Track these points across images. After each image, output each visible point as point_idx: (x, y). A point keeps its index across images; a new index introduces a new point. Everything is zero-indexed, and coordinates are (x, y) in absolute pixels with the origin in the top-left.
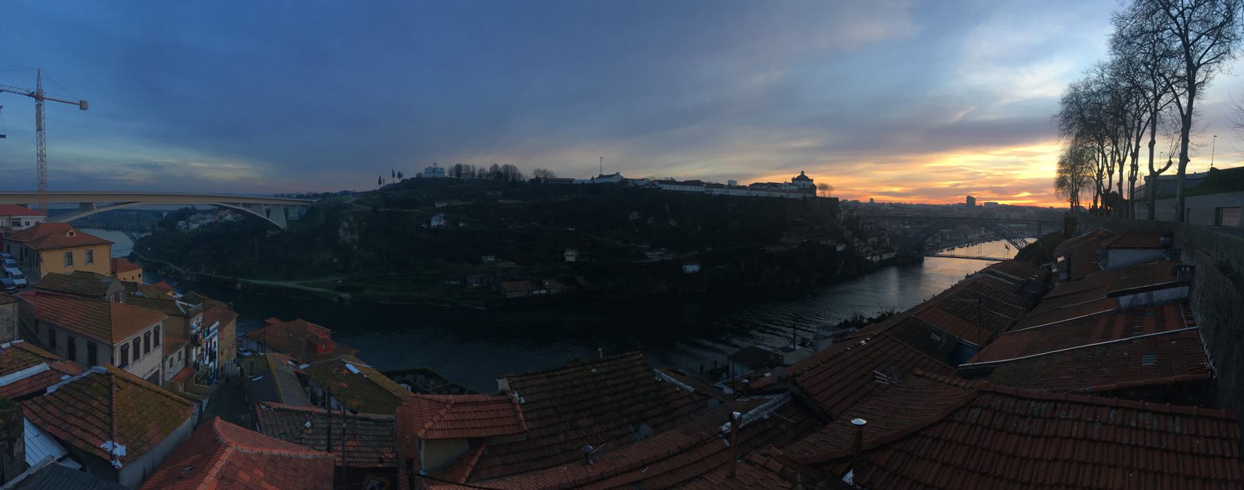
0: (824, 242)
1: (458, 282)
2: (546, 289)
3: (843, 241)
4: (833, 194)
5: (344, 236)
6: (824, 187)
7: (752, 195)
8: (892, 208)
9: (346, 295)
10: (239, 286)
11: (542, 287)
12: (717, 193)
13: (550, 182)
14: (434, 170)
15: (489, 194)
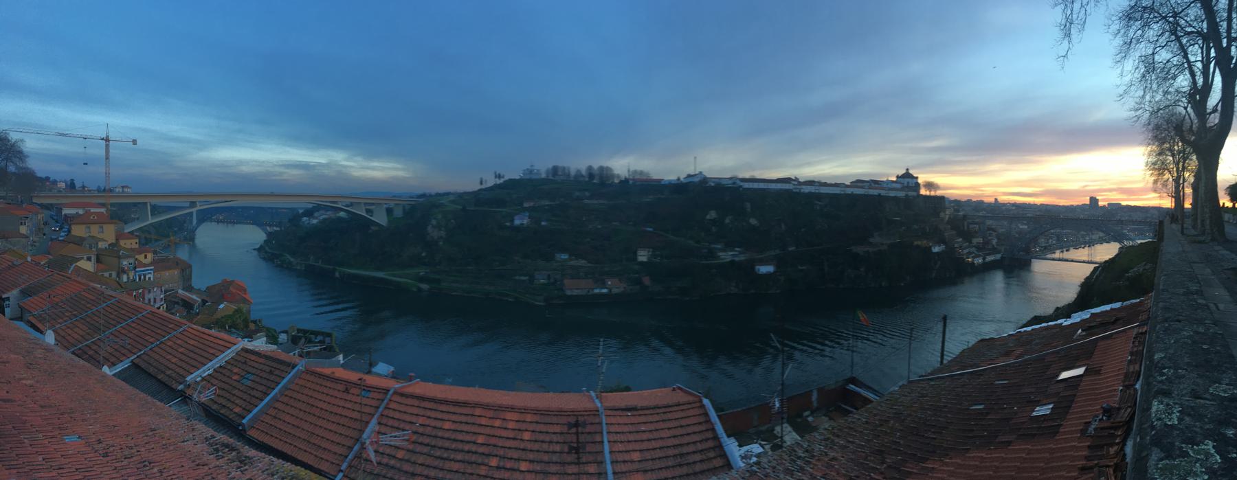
0: (919, 243)
1: (527, 278)
2: (607, 288)
3: (942, 241)
4: (939, 193)
5: (433, 233)
6: (930, 185)
7: (847, 192)
8: (1014, 208)
9: (425, 286)
10: (337, 274)
11: (604, 285)
12: (807, 191)
13: (638, 183)
14: (531, 172)
15: (577, 194)
